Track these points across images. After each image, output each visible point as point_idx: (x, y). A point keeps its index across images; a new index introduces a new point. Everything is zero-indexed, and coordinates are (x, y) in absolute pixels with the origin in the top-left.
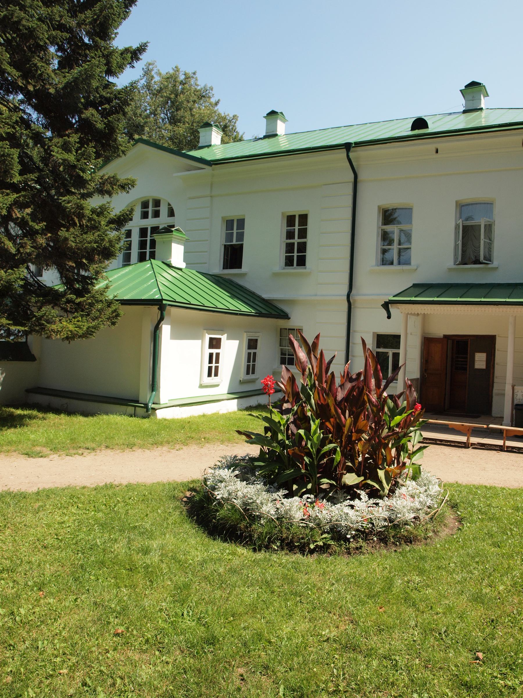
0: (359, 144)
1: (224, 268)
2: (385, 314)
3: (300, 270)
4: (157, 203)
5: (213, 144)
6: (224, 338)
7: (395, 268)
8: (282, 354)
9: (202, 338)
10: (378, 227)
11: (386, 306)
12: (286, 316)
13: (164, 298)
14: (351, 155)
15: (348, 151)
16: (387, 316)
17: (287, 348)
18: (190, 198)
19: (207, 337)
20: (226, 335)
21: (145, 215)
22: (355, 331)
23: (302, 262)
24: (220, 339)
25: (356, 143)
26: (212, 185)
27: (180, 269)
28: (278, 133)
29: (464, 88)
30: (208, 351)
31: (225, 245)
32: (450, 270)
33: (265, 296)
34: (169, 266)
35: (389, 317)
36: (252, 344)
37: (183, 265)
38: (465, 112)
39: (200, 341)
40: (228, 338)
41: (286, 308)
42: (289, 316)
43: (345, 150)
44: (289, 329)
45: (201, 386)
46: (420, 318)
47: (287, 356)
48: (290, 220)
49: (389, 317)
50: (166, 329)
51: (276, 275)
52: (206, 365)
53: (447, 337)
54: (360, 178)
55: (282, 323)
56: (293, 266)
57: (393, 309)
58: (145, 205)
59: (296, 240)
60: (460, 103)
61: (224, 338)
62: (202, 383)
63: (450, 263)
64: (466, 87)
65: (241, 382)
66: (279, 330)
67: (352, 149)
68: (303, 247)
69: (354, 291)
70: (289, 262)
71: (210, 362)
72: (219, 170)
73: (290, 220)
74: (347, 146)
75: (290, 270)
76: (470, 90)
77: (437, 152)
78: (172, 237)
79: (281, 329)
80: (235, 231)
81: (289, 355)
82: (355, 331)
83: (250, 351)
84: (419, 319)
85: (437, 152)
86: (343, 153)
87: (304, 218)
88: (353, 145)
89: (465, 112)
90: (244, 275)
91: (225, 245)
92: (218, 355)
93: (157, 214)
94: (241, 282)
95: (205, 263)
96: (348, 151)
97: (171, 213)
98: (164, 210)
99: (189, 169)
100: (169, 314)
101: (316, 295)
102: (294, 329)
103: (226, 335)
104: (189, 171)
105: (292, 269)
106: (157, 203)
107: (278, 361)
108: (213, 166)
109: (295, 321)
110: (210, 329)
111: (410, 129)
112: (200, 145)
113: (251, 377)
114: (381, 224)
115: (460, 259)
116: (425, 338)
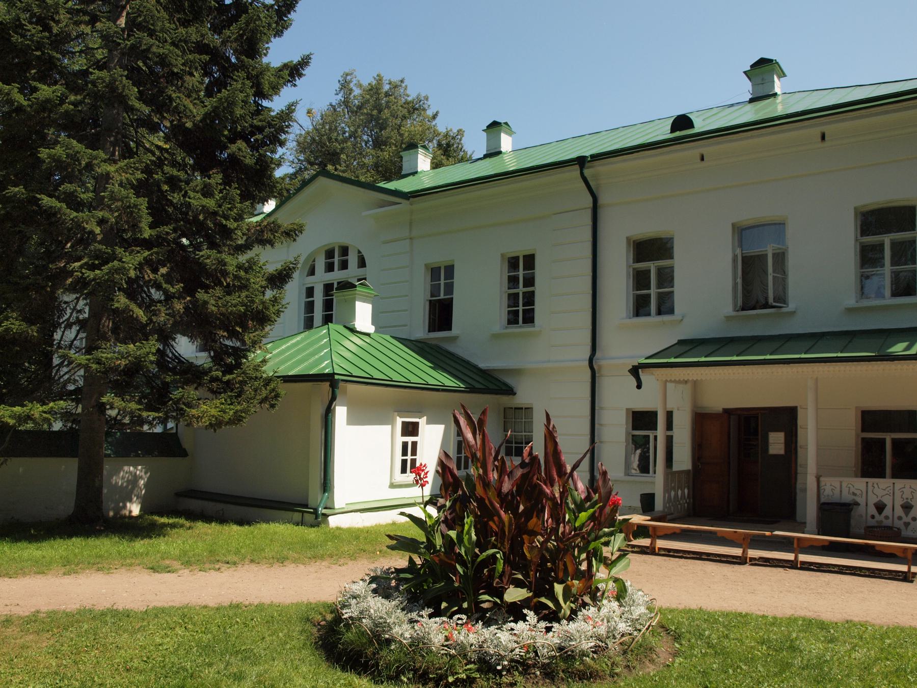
0: (596, 157)
2: (634, 382)
3: (527, 329)
4: (345, 251)
5: (419, 170)
6: (422, 421)
7: (654, 319)
9: (392, 423)
10: (628, 266)
11: (635, 371)
12: (510, 391)
13: (335, 372)
14: (586, 172)
15: (582, 167)
16: (636, 384)
17: (524, 434)
19: (399, 421)
20: (425, 417)
21: (330, 268)
22: (601, 408)
23: (529, 318)
24: (417, 424)
25: (592, 156)
26: (411, 224)
27: (368, 335)
28: (503, 150)
29: (749, 68)
30: (400, 439)
31: (430, 301)
32: (728, 318)
33: (482, 365)
34: (353, 330)
35: (639, 386)
37: (371, 329)
38: (751, 101)
39: (390, 426)
40: (429, 422)
41: (510, 381)
42: (515, 390)
43: (577, 167)
44: (515, 408)
45: (393, 486)
46: (689, 386)
47: (514, 445)
48: (513, 263)
49: (639, 386)
50: (341, 413)
51: (496, 337)
52: (399, 458)
53: (728, 412)
54: (602, 201)
55: (505, 400)
56: (518, 323)
57: (644, 376)
58: (330, 254)
59: (521, 289)
60: (745, 89)
61: (422, 421)
62: (393, 481)
63: (728, 308)
64: (752, 66)
66: (502, 410)
67: (587, 165)
68: (530, 299)
69: (598, 354)
70: (513, 319)
71: (405, 453)
72: (420, 204)
73: (513, 263)
74: (581, 161)
75: (514, 330)
76: (757, 71)
77: (702, 159)
78: (355, 294)
79: (505, 408)
80: (442, 282)
81: (516, 443)
82: (601, 408)
84: (688, 388)
85: (702, 159)
86: (575, 171)
87: (530, 260)
88: (589, 159)
89: (751, 101)
90: (454, 339)
91: (430, 301)
92: (414, 444)
93: (344, 265)
94: (452, 348)
96: (582, 167)
97: (362, 263)
98: (353, 260)
99: (383, 205)
100: (345, 392)
101: (549, 361)
102: (522, 408)
103: (425, 417)
104: (381, 207)
105: (516, 328)
106: (345, 251)
108: (411, 199)
109: (523, 397)
110: (402, 412)
111: (670, 131)
112: (403, 173)
114: (631, 261)
115: (740, 303)
116: (696, 413)
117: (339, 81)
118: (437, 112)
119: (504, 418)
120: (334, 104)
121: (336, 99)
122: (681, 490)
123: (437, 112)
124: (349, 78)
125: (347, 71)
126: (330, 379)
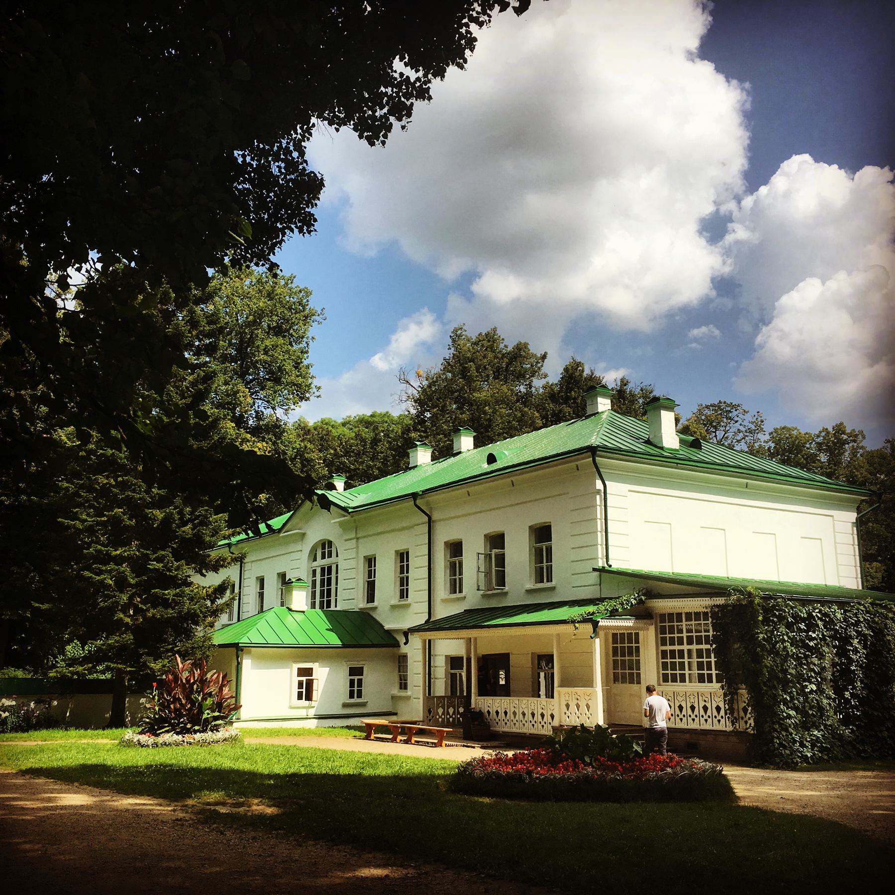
0: (425, 492)
1: (368, 603)
8: (401, 679)
14: (418, 502)
18: (346, 540)
19: (296, 666)
21: (323, 557)
25: (423, 492)
28: (462, 450)
30: (296, 679)
33: (387, 626)
34: (290, 610)
36: (355, 671)
37: (304, 608)
51: (393, 607)
65: (345, 705)
70: (402, 596)
74: (414, 496)
83: (352, 677)
88: (421, 493)
90: (375, 608)
93: (330, 556)
95: (354, 599)
107: (397, 686)
113: (355, 700)
117: (451, 336)
118: (546, 354)
119: (399, 663)
120: (447, 358)
121: (449, 353)
122: (454, 708)
123: (546, 354)
124: (459, 332)
125: (457, 326)
126: (236, 646)
